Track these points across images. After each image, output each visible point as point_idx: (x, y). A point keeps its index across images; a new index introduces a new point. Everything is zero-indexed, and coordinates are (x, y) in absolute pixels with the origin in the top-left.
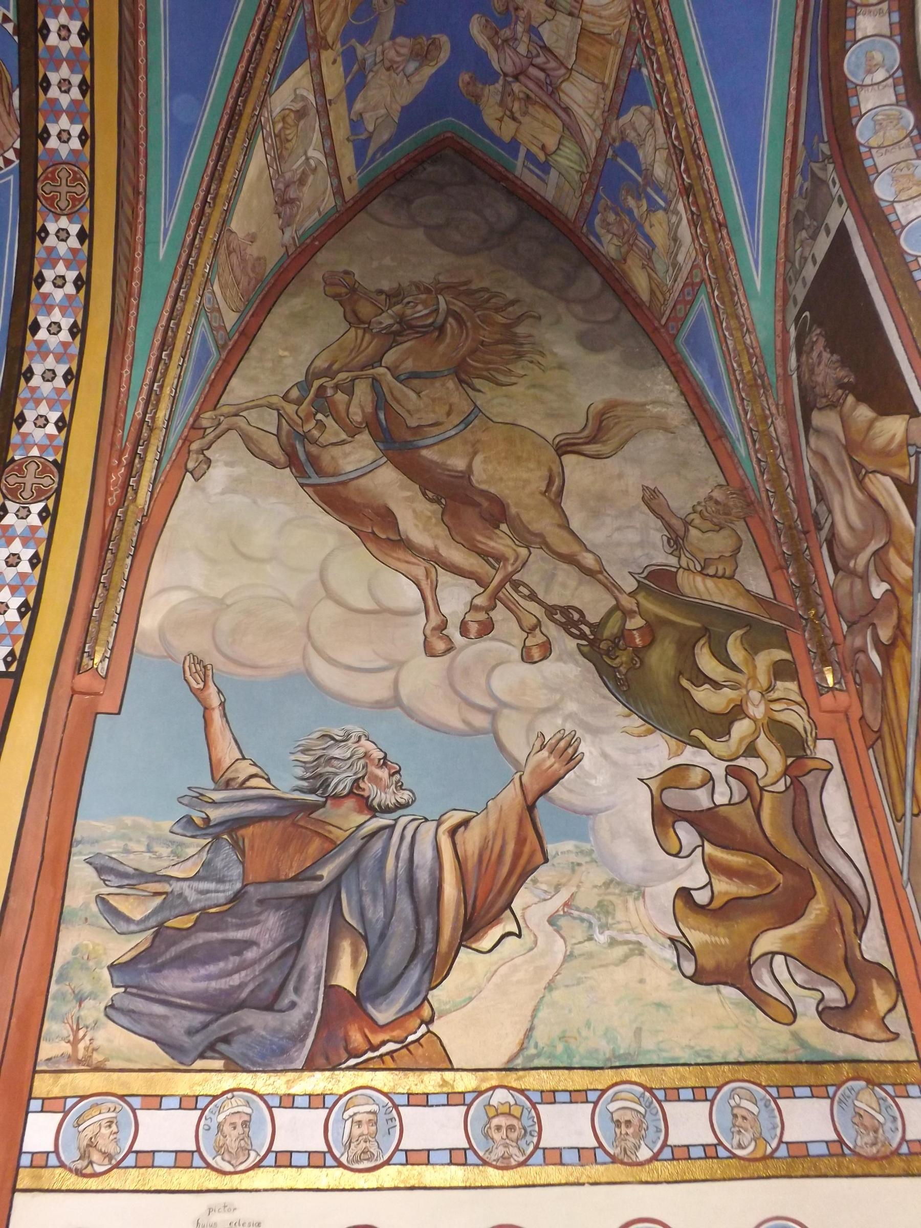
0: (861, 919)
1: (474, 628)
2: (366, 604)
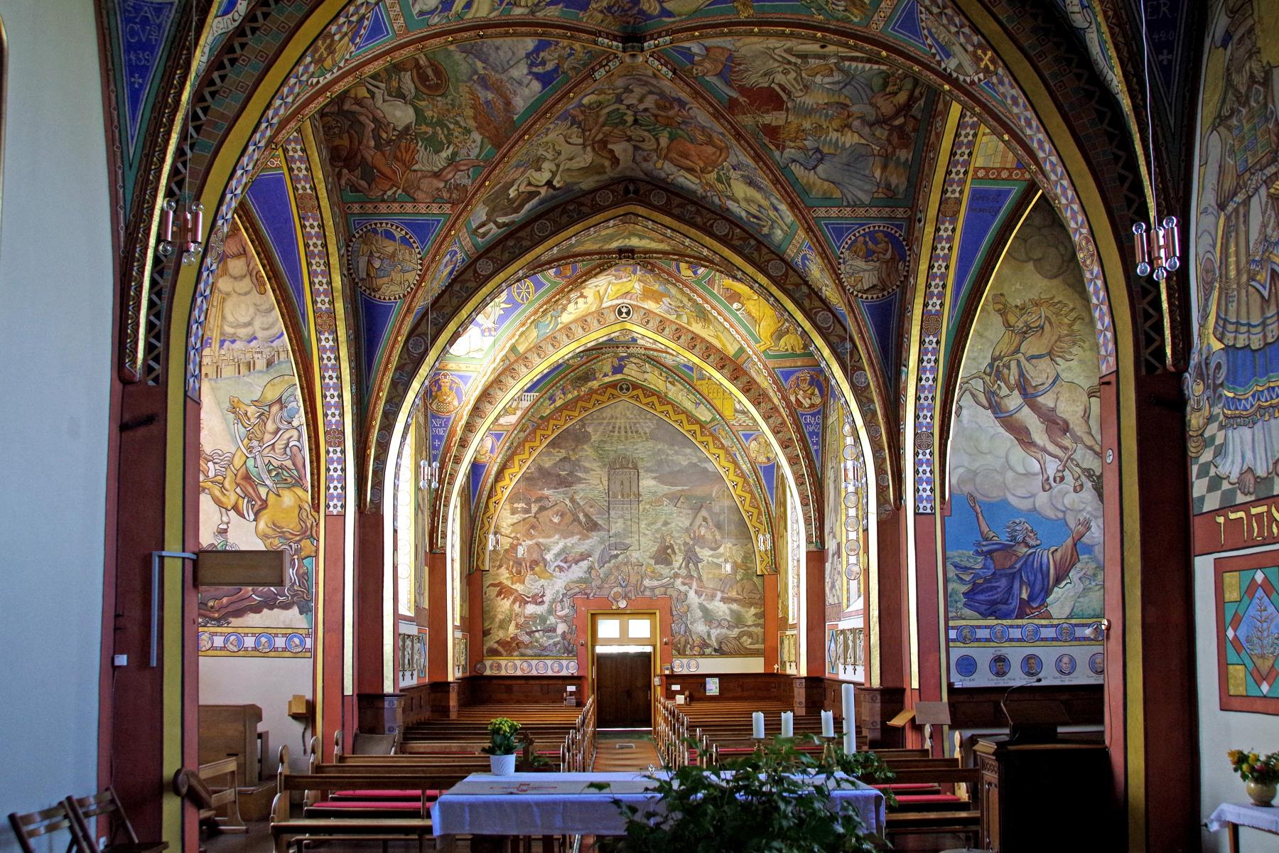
1: (1058, 479)
2: (1024, 472)
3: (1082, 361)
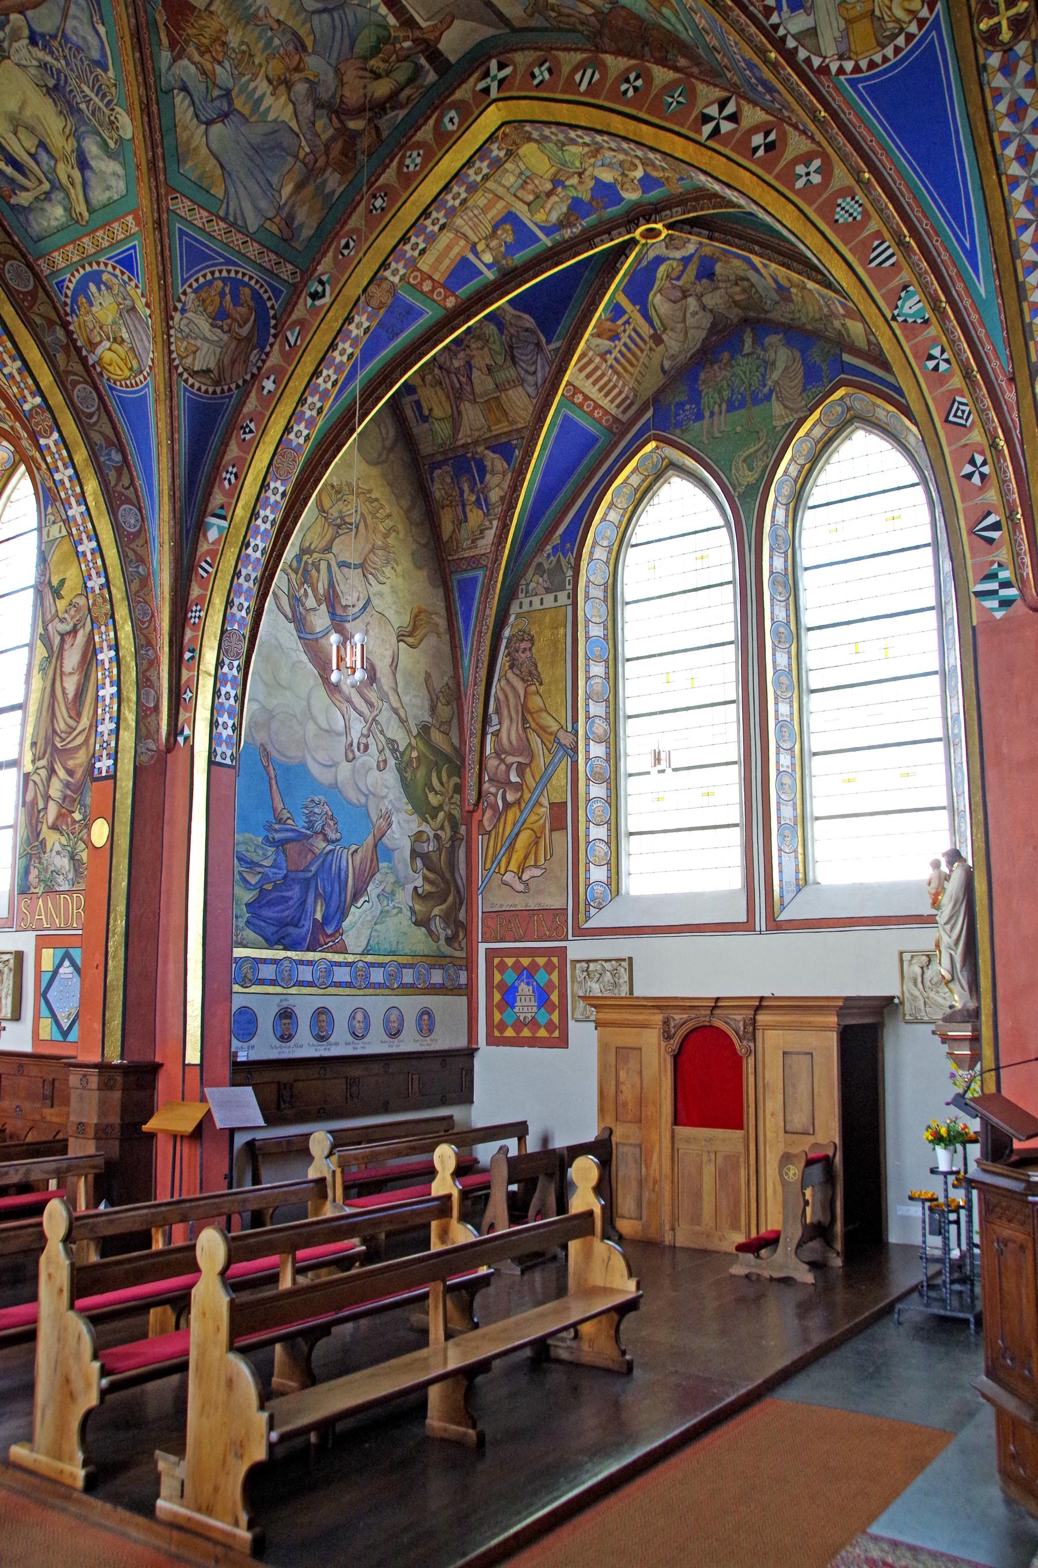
0: (461, 904)
2: (326, 727)
3: (394, 591)
